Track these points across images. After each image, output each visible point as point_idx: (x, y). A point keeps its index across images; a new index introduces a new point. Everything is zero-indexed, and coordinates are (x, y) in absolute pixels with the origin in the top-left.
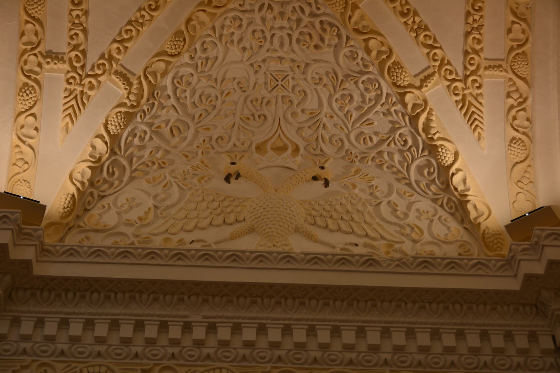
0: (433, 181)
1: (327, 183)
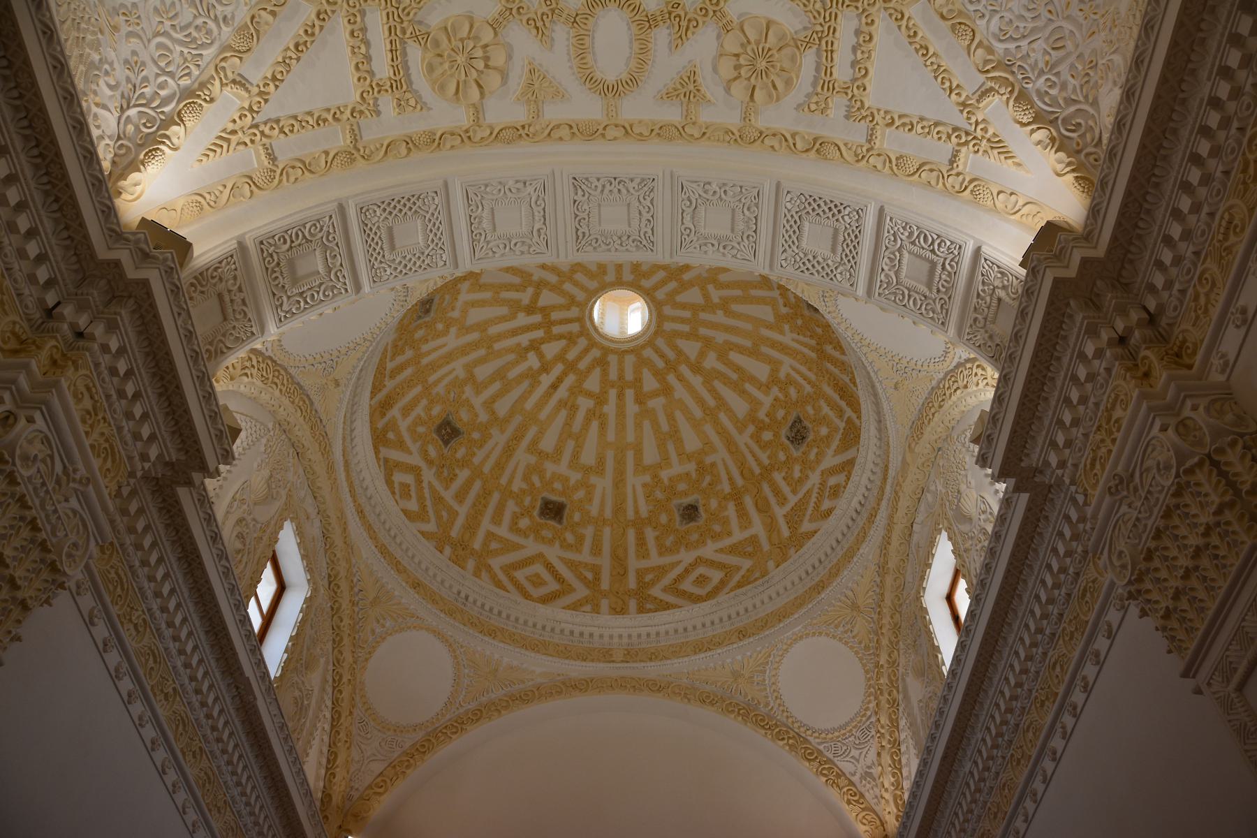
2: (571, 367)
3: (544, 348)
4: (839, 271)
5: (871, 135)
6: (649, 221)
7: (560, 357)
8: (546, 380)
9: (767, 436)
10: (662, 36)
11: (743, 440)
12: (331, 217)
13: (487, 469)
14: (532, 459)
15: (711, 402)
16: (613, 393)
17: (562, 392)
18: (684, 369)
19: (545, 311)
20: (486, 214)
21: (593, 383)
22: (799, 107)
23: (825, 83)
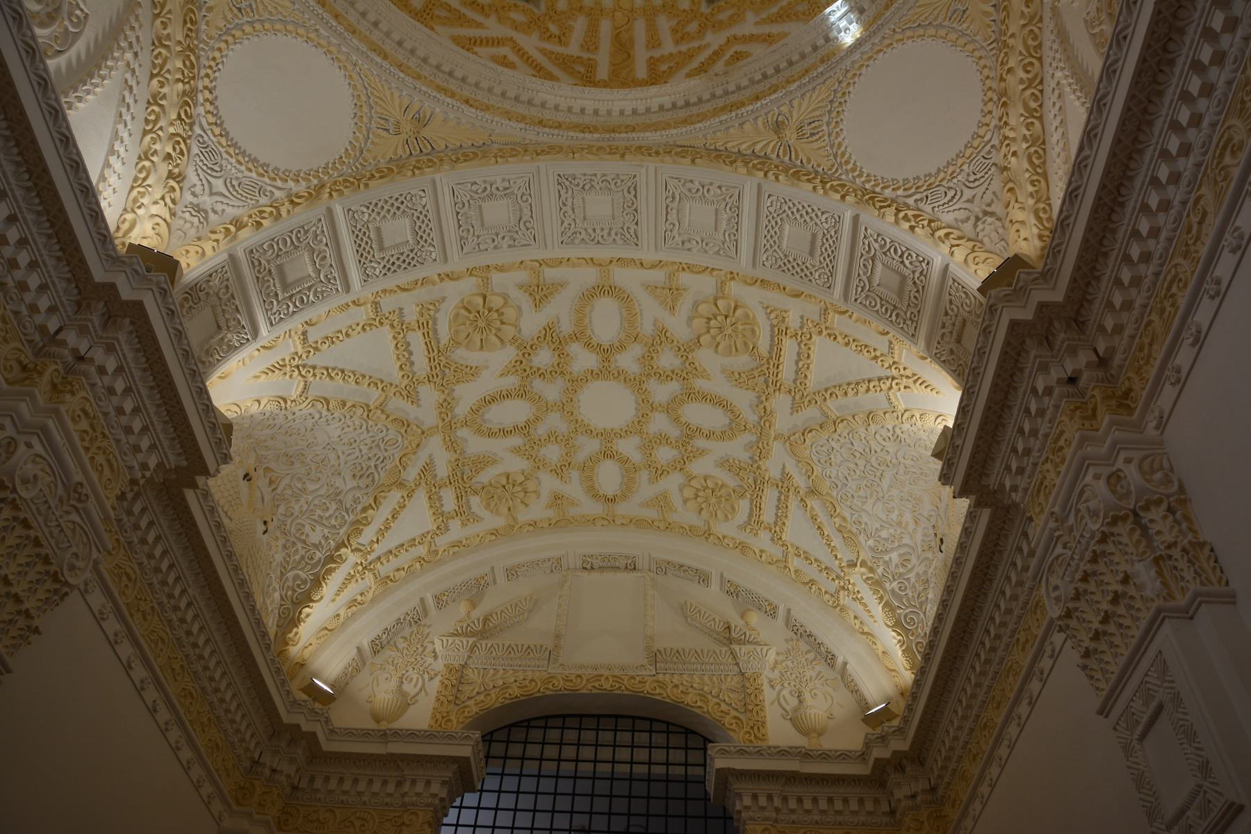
0: (294, 591)
1: (265, 532)
4: (367, 215)
5: (376, 308)
6: (565, 205)
10: (566, 327)
12: (856, 300)
20: (723, 226)
22: (444, 299)
23: (427, 327)
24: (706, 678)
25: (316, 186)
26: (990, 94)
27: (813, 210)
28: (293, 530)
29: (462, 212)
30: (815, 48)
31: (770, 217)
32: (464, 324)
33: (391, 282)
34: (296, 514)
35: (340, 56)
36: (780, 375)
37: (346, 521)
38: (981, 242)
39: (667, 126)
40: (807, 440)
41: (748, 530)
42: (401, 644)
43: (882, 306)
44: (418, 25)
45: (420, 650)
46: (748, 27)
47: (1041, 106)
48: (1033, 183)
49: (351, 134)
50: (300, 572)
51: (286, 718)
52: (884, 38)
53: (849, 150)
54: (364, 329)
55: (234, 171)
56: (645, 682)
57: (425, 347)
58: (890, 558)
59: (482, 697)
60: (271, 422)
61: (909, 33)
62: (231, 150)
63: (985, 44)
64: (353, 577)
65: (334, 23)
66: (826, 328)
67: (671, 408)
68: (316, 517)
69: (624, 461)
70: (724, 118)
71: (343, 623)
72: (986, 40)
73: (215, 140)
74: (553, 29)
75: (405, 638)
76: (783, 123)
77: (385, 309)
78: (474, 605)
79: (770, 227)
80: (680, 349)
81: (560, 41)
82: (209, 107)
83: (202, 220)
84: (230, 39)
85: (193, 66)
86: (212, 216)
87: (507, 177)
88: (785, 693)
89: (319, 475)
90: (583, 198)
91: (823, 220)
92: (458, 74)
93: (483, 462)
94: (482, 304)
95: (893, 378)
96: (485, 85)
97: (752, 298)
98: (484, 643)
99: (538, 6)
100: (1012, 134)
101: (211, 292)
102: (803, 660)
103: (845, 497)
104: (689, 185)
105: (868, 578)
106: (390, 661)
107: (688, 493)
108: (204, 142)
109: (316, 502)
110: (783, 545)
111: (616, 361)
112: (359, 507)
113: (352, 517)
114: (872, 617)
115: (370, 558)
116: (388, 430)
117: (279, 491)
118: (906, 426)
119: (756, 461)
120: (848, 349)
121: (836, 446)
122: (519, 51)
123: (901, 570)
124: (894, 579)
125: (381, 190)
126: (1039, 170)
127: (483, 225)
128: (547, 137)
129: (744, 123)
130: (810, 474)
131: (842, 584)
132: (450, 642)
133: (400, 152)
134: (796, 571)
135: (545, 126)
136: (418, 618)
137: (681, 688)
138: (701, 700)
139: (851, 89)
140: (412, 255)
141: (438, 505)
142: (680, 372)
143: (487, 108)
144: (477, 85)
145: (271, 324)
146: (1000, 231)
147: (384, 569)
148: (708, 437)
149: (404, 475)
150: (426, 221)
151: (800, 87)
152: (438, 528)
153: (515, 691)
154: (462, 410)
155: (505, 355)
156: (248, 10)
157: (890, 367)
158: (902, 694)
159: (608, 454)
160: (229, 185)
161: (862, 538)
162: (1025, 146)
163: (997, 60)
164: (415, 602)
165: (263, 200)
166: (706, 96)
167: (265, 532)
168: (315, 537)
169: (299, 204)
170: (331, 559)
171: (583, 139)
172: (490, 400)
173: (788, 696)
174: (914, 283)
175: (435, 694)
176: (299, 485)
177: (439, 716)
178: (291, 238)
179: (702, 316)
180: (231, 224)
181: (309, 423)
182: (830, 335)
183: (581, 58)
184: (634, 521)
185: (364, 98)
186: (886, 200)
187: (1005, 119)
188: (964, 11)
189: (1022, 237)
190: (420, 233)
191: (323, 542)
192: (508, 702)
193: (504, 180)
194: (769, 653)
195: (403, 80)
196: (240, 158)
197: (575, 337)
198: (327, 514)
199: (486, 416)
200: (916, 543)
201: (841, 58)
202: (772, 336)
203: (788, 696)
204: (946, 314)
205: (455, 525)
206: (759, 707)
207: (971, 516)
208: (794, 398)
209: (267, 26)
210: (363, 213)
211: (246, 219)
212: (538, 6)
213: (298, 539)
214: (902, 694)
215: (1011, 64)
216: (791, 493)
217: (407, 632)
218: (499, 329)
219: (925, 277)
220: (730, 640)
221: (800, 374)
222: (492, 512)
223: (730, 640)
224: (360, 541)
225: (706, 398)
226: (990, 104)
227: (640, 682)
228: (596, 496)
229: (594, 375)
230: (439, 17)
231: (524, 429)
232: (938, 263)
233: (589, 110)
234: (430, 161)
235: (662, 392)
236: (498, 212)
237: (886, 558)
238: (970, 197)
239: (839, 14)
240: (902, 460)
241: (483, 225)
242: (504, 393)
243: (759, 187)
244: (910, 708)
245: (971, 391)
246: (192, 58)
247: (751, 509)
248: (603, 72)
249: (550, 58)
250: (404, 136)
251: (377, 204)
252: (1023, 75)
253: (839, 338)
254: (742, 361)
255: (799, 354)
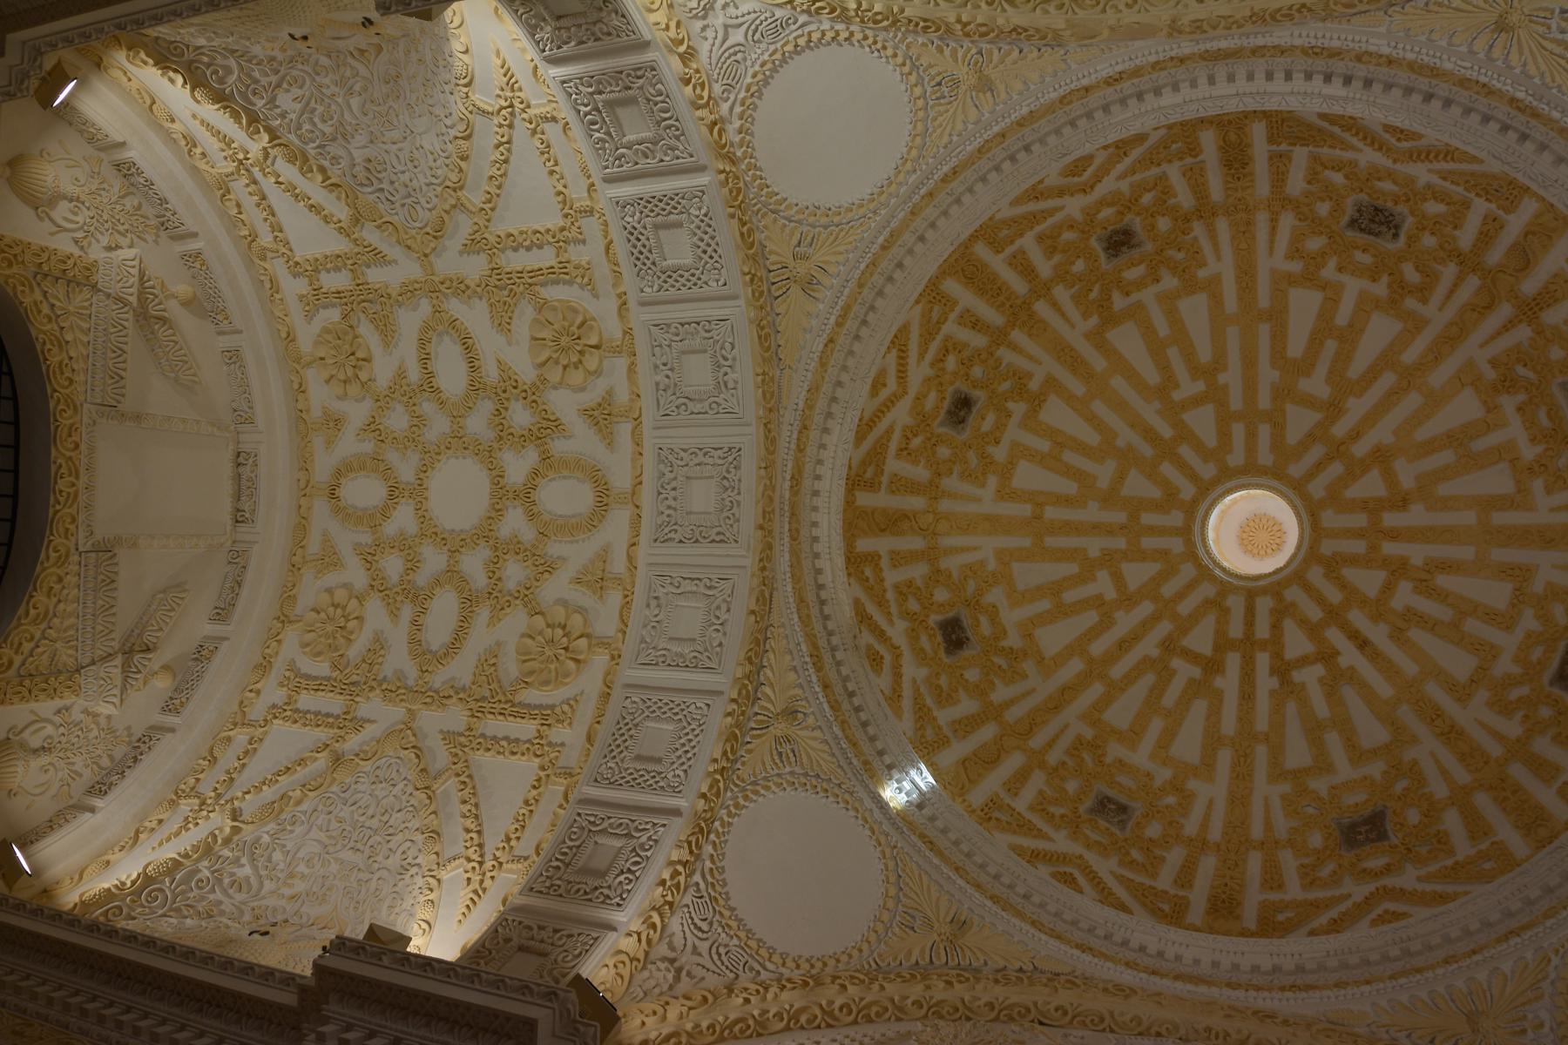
0: (209, 65)
1: (292, 36)
2: (1334, 615)
3: (1290, 654)
4: (697, 213)
6: (705, 454)
7: (1313, 631)
8: (1349, 656)
9: (1410, 274)
10: (559, 447)
11: (1437, 314)
12: (579, 814)
13: (1462, 776)
14: (1482, 695)
15: (1388, 379)
16: (1389, 548)
17: (1378, 634)
18: (1340, 430)
19: (1222, 644)
20: (676, 648)
21: (1369, 581)
22: (596, 296)
23: (562, 273)
24: (72, 620)
25: (734, 154)
26: (819, 965)
27: (689, 759)
28: (295, 73)
29: (700, 328)
30: (881, 753)
31: (683, 706)
32: (564, 319)
33: (616, 234)
34: (318, 79)
35: (885, 195)
36: (491, 716)
37: (306, 143)
38: (644, 968)
39: (796, 578)
40: (406, 752)
41: (287, 674)
42: (130, 203)
43: (570, 848)
44: (920, 289)
45: (121, 228)
46: (912, 671)
47: (802, 1028)
48: (711, 1026)
49: (795, 201)
50: (235, 76)
51: (14, 38)
52: (887, 835)
53: (761, 799)
54: (559, 193)
55: (754, 56)
56: (67, 538)
57: (536, 268)
58: (243, 866)
59: (46, 310)
60: (441, 63)
61: (891, 864)
62: (778, 56)
63: (875, 955)
64: (229, 145)
65: (923, 192)
66: (548, 776)
67: (452, 575)
68: (313, 104)
69: (385, 512)
70: (804, 647)
71: (162, 127)
72: (880, 955)
73: (791, 38)
74: (916, 442)
75: (139, 207)
76: (795, 719)
77: (584, 222)
78: (186, 304)
79: (672, 705)
80: (528, 589)
81: (901, 450)
82: (830, 35)
83: (694, 12)
84: (906, 69)
85: (876, 22)
86: (699, 24)
87: (739, 386)
88: (50, 730)
89: (371, 115)
90: (712, 477)
91: (677, 772)
92: (864, 332)
93: (387, 331)
94: (589, 343)
95: (481, 863)
96: (851, 362)
97: (589, 682)
98: (130, 316)
99: (942, 424)
100: (770, 996)
101: (604, 14)
102: (98, 752)
103: (329, 802)
104: (724, 607)
105: (216, 836)
106: (105, 186)
107: (340, 596)
108: (788, 25)
109: (333, 107)
110: (266, 720)
111: (515, 507)
112: (326, 163)
113: (313, 152)
114: (161, 844)
115: (256, 170)
116: (430, 210)
117: (350, 60)
118: (420, 881)
119: (381, 685)
120: (521, 803)
121: (396, 791)
122: (892, 401)
123: (226, 881)
124: (213, 872)
125: (726, 233)
126: (727, 1032)
127: (684, 353)
128: (787, 435)
129: (796, 672)
130: (362, 755)
131: (209, 801)
132: (131, 270)
133: (773, 258)
134: (229, 739)
135: (800, 432)
136: (168, 226)
137: (57, 587)
138: (38, 615)
139: (831, 799)
140: (648, 263)
141: (329, 266)
142: (498, 588)
143: (823, 364)
144: (851, 353)
145: (564, 82)
146: (657, 991)
147: (239, 186)
148: (414, 622)
149: (370, 225)
150: (689, 284)
151: (836, 738)
152: (297, 263)
153: (54, 359)
154: (455, 307)
155: (524, 368)
156: (938, 95)
157: (496, 858)
158: (45, 891)
159: (394, 492)
160: (737, 48)
161: (272, 827)
162: (756, 1013)
163: (858, 971)
164: (191, 225)
165: (718, 89)
166: (831, 625)
167: (292, 36)
168: (285, 101)
169: (711, 133)
170: (253, 119)
171: (784, 478)
172: (467, 344)
173: (44, 734)
174: (596, 888)
175: (53, 246)
176: (357, 88)
177: (17, 250)
178: (670, 118)
179: (567, 618)
180: (689, 47)
181: (438, 111)
182: (539, 780)
183: (882, 474)
184: (304, 522)
185: (836, 219)
186: (699, 847)
187: (789, 986)
188: (913, 928)
189: (646, 1020)
190: (674, 275)
191: (278, 111)
192: (38, 347)
193: (736, 382)
194: (111, 707)
195: (858, 268)
196: (769, 66)
197: (546, 457)
198: (316, 120)
199: (446, 338)
200: (264, 898)
201: (867, 786)
202: (540, 707)
203: (44, 734)
204: (556, 931)
205: (301, 286)
206: (27, 694)
207: (289, 979)
208: (461, 734)
209: (921, 114)
210: (700, 209)
211: (694, 66)
212: (942, 424)
213: (283, 79)
214: (45, 891)
215: (852, 989)
216: (336, 731)
217: (149, 211)
218: (557, 362)
219: (603, 902)
220: (128, 652)
221: (493, 743)
222: (319, 336)
223: (128, 652)
224: (279, 161)
225: (465, 620)
226: (807, 966)
227: (67, 530)
228: (339, 473)
229: (498, 478)
230: (931, 310)
231: (429, 385)
232: (619, 917)
233: (818, 485)
234: (761, 294)
235: (474, 564)
236: (698, 373)
237: (244, 860)
238: (699, 950)
239: (918, 780)
240: (378, 875)
241: (684, 353)
242: (477, 363)
243: (721, 693)
244: (20, 906)
245: (452, 973)
246: (885, 23)
247: (316, 678)
248: (864, 499)
249: (882, 437)
250: (791, 264)
251: (710, 226)
252: (837, 1005)
253: (534, 792)
254: (511, 668)
255: (517, 741)
